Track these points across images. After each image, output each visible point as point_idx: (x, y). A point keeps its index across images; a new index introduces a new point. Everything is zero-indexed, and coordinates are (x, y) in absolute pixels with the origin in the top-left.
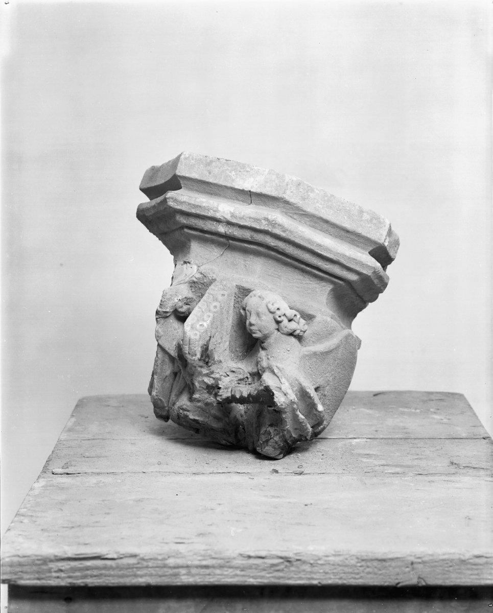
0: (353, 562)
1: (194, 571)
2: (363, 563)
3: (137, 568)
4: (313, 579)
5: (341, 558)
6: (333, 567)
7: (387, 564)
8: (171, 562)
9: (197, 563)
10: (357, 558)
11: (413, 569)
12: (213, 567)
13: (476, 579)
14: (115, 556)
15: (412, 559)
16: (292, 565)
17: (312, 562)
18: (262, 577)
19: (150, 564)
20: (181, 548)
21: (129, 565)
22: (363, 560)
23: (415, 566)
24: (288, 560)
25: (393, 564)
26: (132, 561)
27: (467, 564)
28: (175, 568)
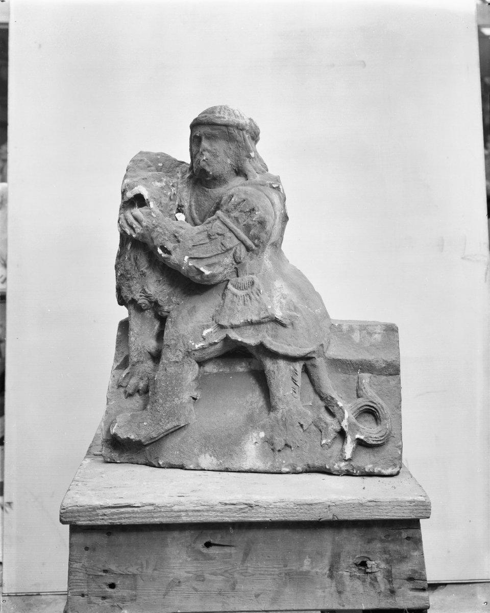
0: (292, 506)
1: (190, 514)
2: (298, 507)
3: (153, 512)
4: (266, 517)
5: (284, 504)
6: (279, 509)
7: (313, 507)
8: (176, 508)
9: (193, 508)
10: (295, 504)
11: (330, 510)
12: (203, 511)
13: (369, 515)
14: (140, 505)
15: (329, 503)
16: (253, 509)
17: (266, 506)
18: (234, 517)
19: (162, 510)
20: (182, 499)
21: (148, 510)
22: (298, 505)
23: (331, 508)
24: (251, 506)
25: (317, 507)
26: (151, 508)
27: (363, 506)
28: (178, 512)
